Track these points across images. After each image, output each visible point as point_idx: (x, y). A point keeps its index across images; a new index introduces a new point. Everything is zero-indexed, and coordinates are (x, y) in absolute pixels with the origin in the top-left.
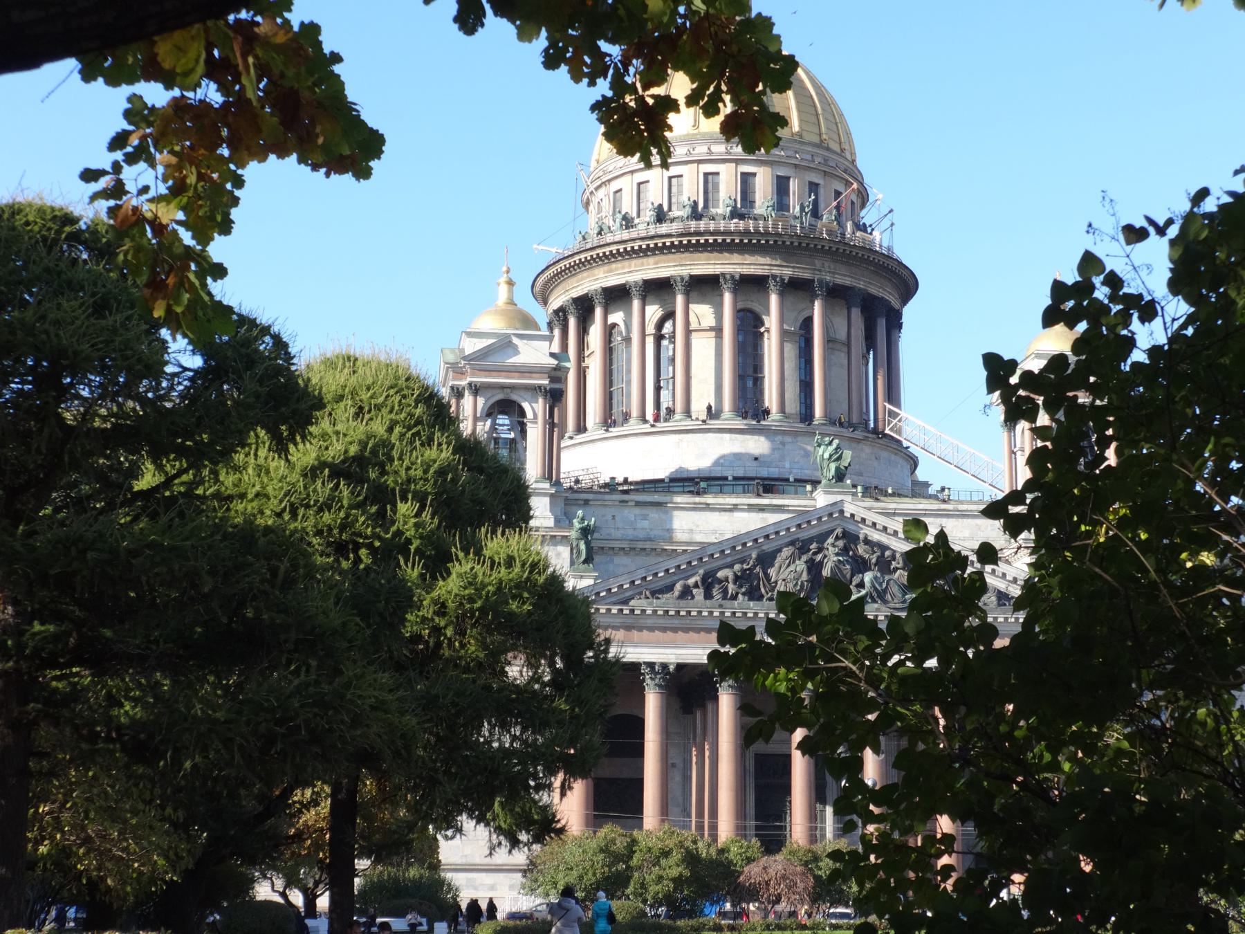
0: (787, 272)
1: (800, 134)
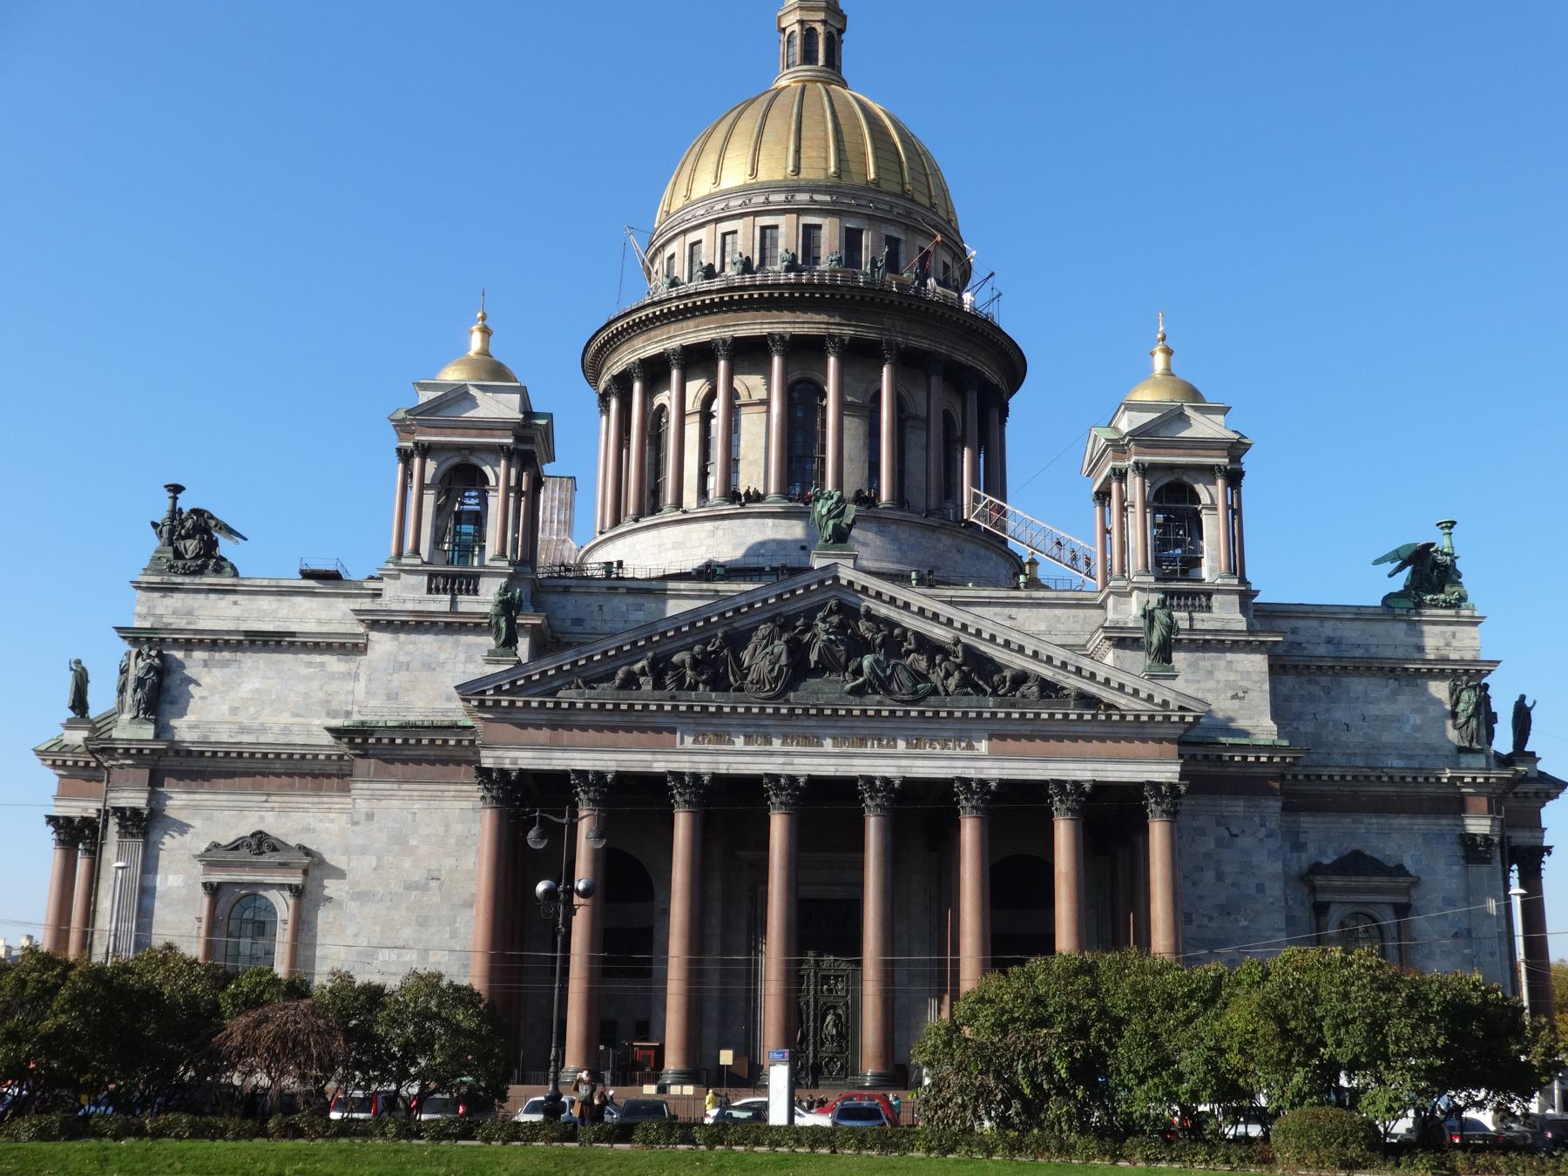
0: (848, 331)
1: (876, 182)
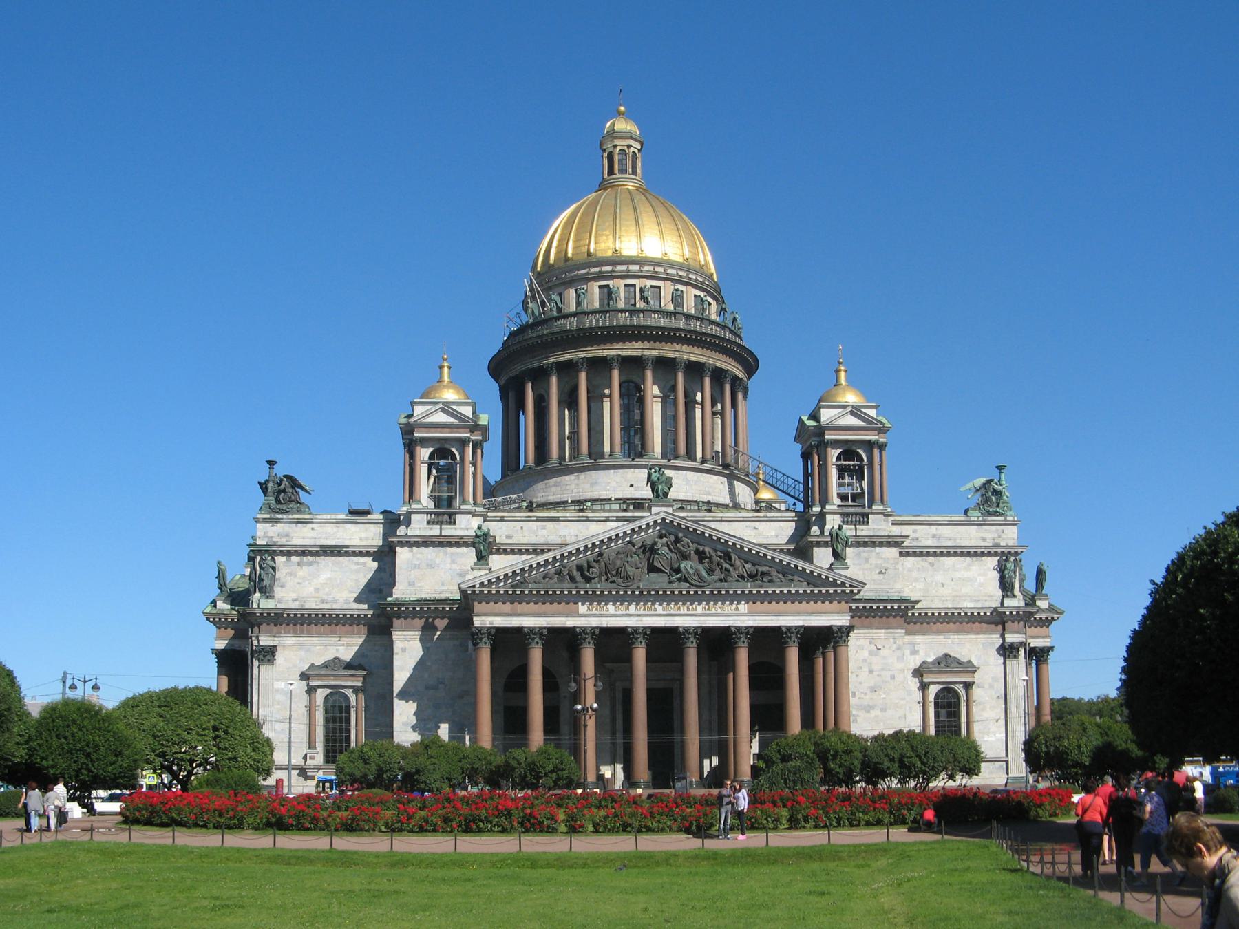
0: (655, 353)
